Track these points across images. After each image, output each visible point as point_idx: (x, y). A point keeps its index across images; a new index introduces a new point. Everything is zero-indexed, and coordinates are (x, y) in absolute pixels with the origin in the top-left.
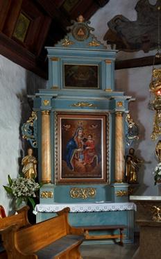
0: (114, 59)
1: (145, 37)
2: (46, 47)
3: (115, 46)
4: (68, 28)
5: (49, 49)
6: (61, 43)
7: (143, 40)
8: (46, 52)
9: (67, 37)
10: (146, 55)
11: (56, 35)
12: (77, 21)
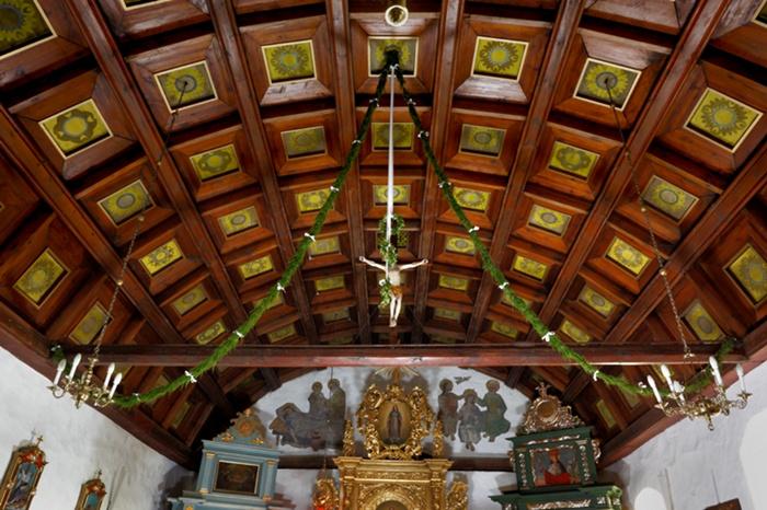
0: (278, 460)
1: (316, 433)
4: (232, 421)
10: (316, 453)
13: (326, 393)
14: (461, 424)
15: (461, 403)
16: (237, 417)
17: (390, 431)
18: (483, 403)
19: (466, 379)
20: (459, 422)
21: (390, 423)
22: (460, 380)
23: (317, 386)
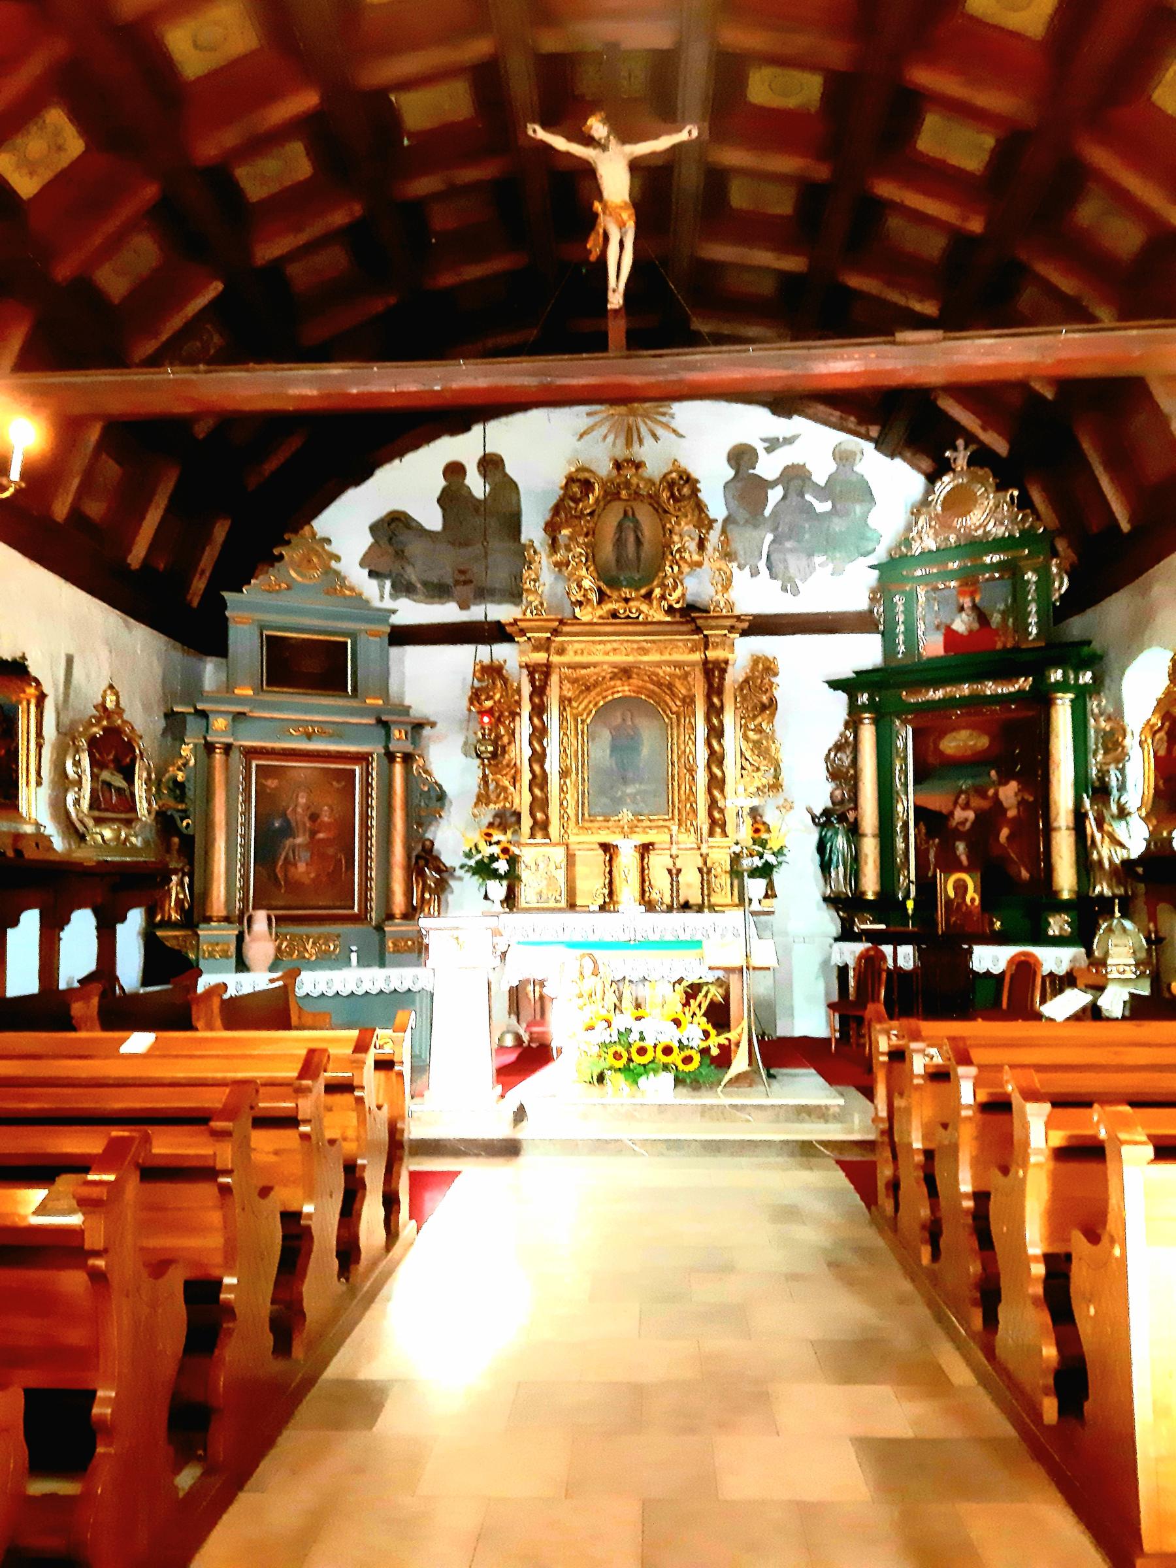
1: (462, 572)
3: (388, 583)
4: (276, 552)
7: (463, 578)
8: (223, 605)
13: (476, 485)
14: (773, 541)
15: (775, 495)
16: (288, 543)
17: (618, 561)
18: (824, 492)
19: (789, 441)
20: (769, 537)
21: (619, 543)
22: (773, 445)
23: (454, 471)
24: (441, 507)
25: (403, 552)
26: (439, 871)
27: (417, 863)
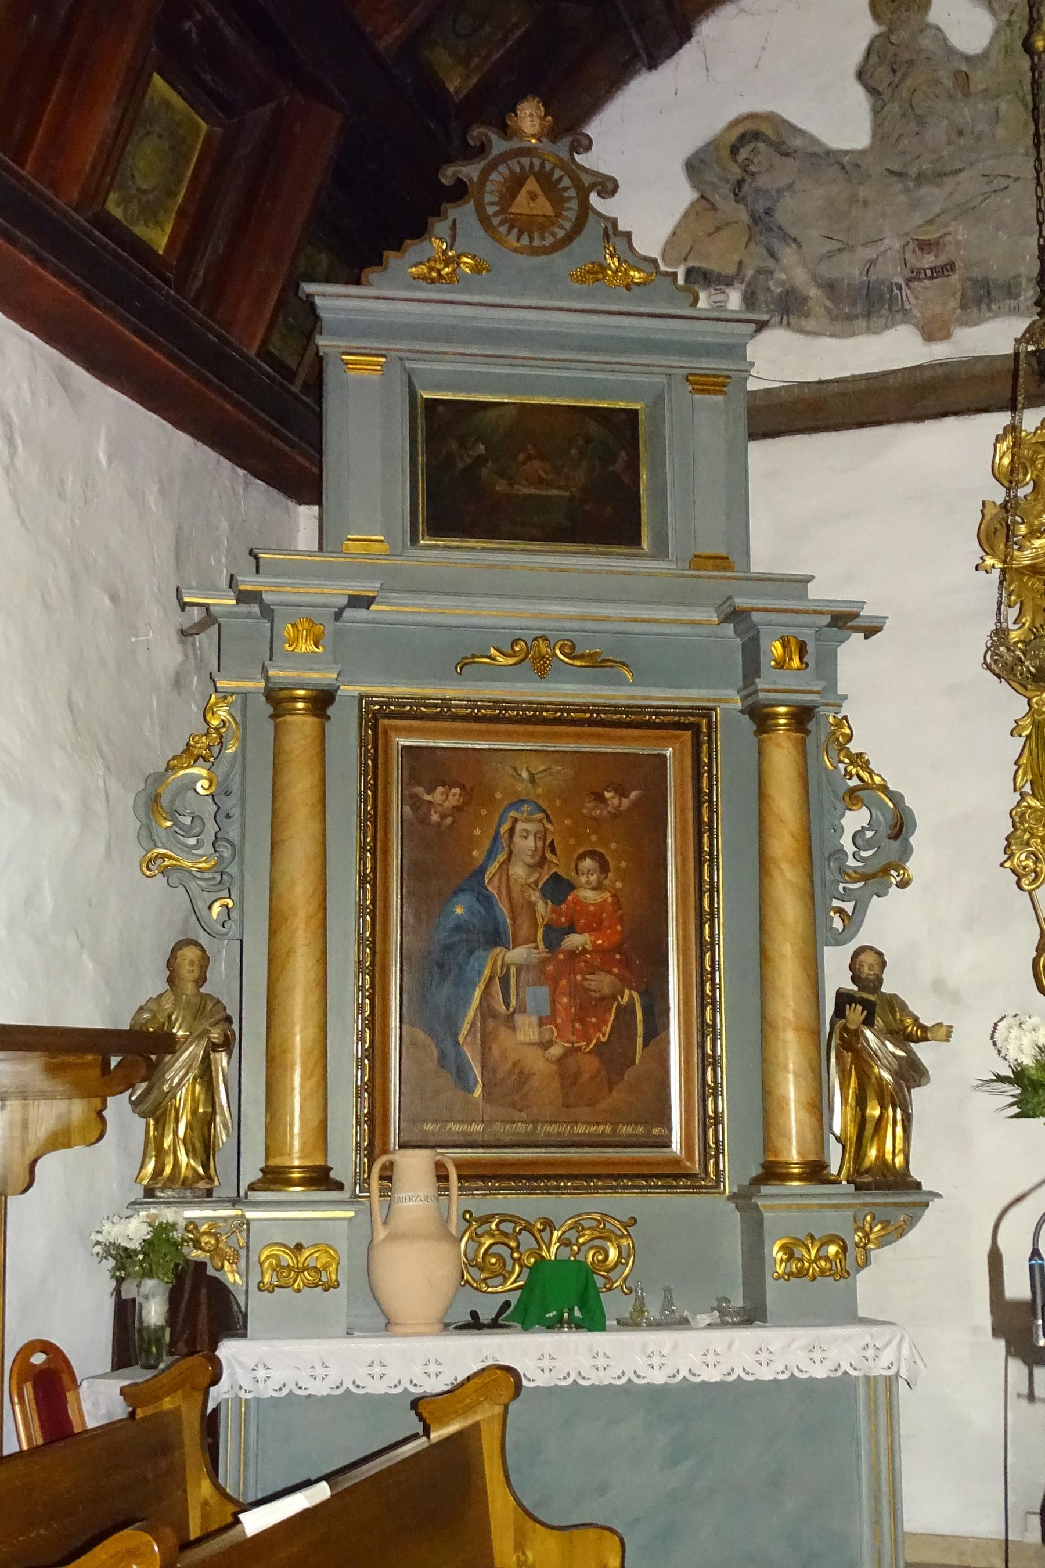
1: (925, 246)
2: (309, 288)
4: (448, 175)
5: (331, 299)
6: (408, 263)
7: (929, 261)
8: (310, 319)
9: (441, 227)
10: (939, 352)
11: (376, 218)
12: (506, 131)
24: (872, 91)
25: (768, 212)
26: (903, 1037)
27: (840, 1012)
